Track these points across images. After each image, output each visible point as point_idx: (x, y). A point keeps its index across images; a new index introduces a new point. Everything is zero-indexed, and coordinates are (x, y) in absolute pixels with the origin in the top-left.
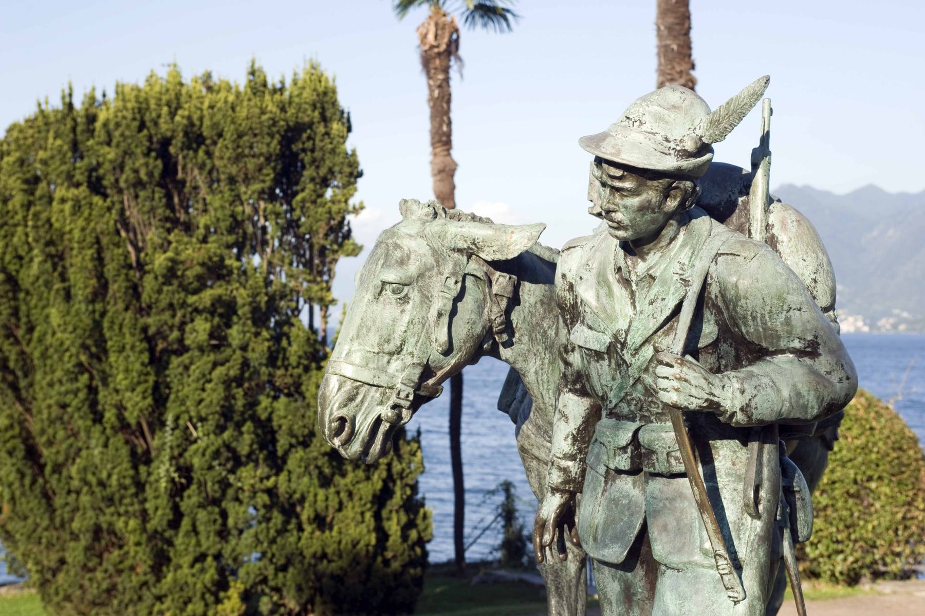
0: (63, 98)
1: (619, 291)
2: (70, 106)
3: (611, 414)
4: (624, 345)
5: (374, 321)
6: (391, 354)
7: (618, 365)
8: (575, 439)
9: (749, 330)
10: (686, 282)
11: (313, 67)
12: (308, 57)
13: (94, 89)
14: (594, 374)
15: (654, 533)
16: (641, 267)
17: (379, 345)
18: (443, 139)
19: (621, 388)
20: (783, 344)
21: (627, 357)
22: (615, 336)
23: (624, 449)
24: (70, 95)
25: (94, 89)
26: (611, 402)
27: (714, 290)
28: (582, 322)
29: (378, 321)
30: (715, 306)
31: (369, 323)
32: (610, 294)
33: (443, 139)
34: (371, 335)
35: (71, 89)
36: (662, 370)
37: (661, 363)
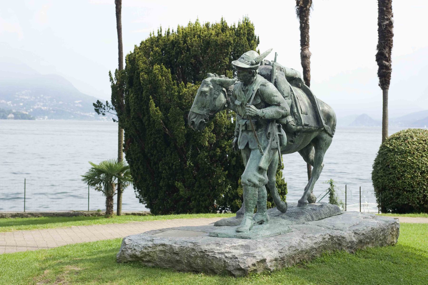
0: (158, 32)
1: (243, 93)
2: (160, 35)
6: (204, 107)
9: (266, 100)
10: (254, 91)
11: (246, 20)
12: (244, 16)
13: (169, 29)
18: (304, 42)
20: (273, 103)
22: (242, 102)
23: (244, 125)
24: (161, 31)
25: (169, 29)
27: (259, 92)
30: (260, 96)
32: (241, 93)
33: (304, 42)
35: (161, 29)
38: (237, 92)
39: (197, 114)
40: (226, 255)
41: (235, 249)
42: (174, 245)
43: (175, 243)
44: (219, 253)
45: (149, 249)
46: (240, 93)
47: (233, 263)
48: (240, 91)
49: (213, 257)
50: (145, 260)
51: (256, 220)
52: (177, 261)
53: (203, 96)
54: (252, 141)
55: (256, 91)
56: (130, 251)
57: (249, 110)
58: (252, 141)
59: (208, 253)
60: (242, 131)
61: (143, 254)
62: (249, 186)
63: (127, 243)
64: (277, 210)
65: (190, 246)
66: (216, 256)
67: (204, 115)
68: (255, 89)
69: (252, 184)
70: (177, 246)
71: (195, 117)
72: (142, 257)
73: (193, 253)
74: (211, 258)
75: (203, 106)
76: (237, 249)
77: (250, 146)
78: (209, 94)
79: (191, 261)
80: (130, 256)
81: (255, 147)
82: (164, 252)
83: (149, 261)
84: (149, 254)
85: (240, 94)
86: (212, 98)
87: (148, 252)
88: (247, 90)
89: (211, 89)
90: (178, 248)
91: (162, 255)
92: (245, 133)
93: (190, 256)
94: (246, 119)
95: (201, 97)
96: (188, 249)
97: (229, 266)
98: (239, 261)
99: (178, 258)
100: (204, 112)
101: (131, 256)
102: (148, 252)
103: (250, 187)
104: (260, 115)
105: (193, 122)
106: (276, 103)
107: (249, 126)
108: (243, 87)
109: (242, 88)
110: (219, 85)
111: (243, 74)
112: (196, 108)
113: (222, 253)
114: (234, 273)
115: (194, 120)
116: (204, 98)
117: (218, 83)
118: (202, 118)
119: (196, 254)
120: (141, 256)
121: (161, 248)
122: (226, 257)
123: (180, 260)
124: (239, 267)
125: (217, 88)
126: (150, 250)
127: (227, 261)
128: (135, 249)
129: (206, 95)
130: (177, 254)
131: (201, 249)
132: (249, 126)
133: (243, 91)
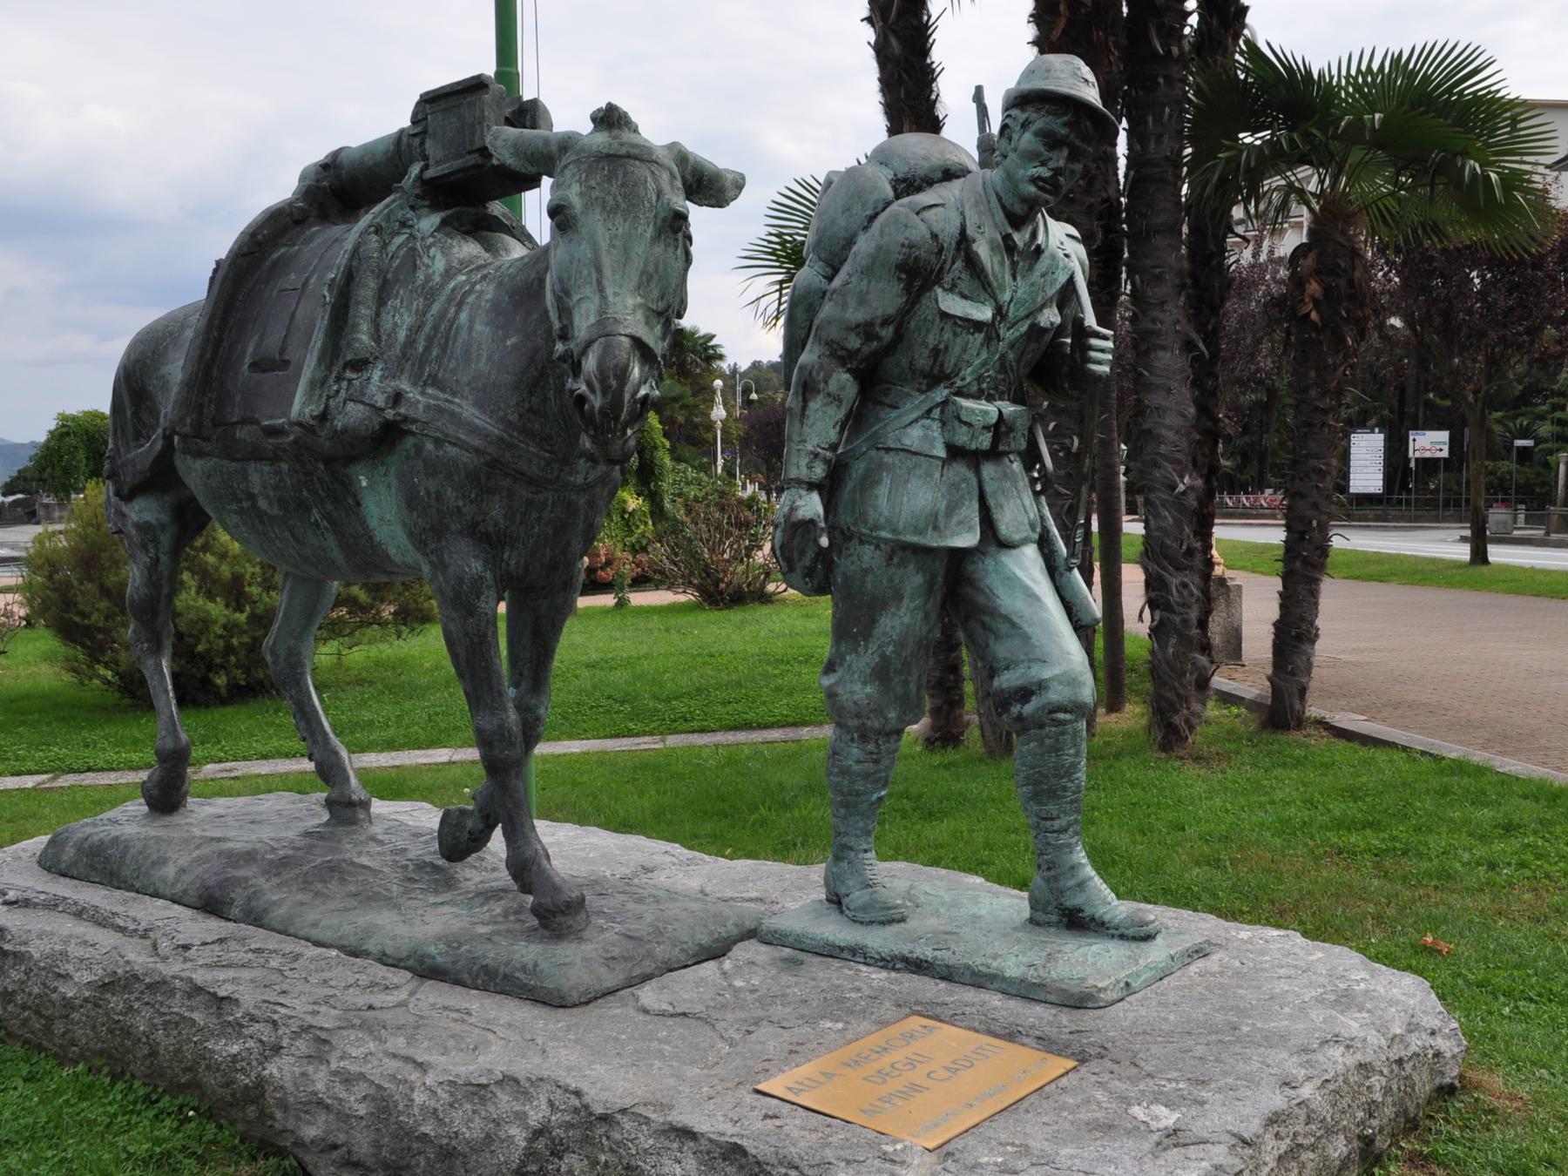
19: (983, 364)
21: (1001, 332)
26: (963, 379)
29: (661, 268)
31: (651, 269)
34: (653, 285)
95: (659, 249)
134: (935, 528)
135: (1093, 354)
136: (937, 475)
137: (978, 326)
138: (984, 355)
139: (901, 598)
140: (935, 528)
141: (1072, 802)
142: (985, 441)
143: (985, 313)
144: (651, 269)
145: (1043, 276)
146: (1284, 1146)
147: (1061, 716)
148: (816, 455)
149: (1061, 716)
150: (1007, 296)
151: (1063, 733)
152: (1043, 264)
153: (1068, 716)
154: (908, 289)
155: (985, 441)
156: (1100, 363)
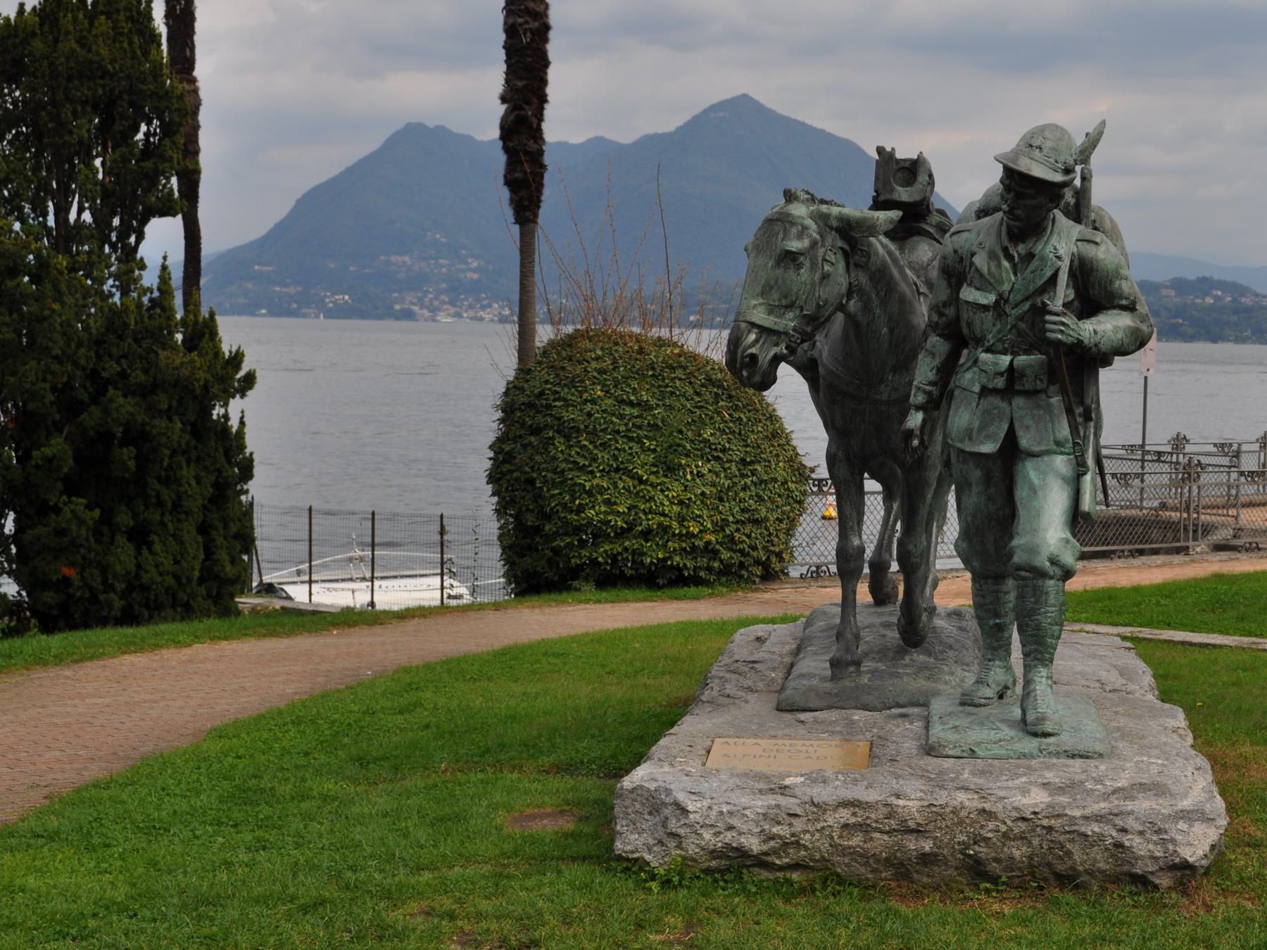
1: (1006, 264)
3: (988, 351)
4: (1007, 301)
5: (776, 282)
7: (999, 316)
8: (938, 370)
10: (1059, 258)
14: (978, 322)
15: (1020, 432)
16: (1022, 248)
17: (779, 300)
19: (1000, 331)
20: (1116, 302)
22: (1000, 296)
23: (1001, 374)
28: (970, 285)
31: (772, 283)
32: (999, 265)
36: (1048, 317)
37: (1051, 313)
38: (980, 261)
39: (763, 330)
40: (1119, 822)
41: (1125, 798)
42: (901, 802)
43: (898, 796)
44: (1085, 818)
45: (795, 821)
46: (993, 264)
47: (1151, 847)
48: (992, 256)
49: (1069, 832)
50: (778, 862)
51: (993, 686)
52: (926, 859)
53: (786, 268)
54: (1028, 428)
55: (1067, 262)
56: (707, 835)
57: (1063, 324)
58: (1028, 428)
59: (1045, 822)
60: (985, 391)
61: (772, 843)
62: (1052, 578)
63: (690, 808)
64: (897, 636)
65: (967, 803)
66: (1083, 829)
67: (786, 334)
68: (1061, 252)
69: (1058, 572)
70: (910, 803)
71: (756, 341)
72: (766, 854)
73: (991, 825)
74: (1062, 838)
75: (784, 302)
76: (1133, 798)
77: (1024, 442)
78: (807, 264)
79: (982, 850)
80: (713, 851)
81: (1044, 448)
82: (864, 828)
83: (795, 866)
84: (797, 843)
85: (993, 269)
86: (817, 277)
87: (793, 835)
88: (1030, 256)
89: (814, 244)
90: (918, 811)
91: (856, 841)
92: (995, 400)
93: (978, 839)
94: (1005, 353)
95: (779, 272)
96: (963, 814)
97: (1137, 858)
98: (1173, 841)
99: (927, 846)
100: (789, 322)
101: (714, 854)
102: (793, 835)
103: (1052, 582)
104: (1086, 342)
105: (754, 357)
106: (1124, 302)
107: (1023, 375)
108: (1006, 243)
109: (1005, 250)
110: (837, 230)
111: (1034, 202)
112: (761, 309)
113: (1099, 818)
114: (1158, 882)
115: (753, 350)
116: (791, 273)
117: (835, 224)
118: (777, 345)
119: (1003, 828)
120: (765, 848)
121: (845, 815)
122: (1124, 830)
123: (936, 855)
124: (1177, 860)
125: (829, 241)
126: (799, 825)
127: (1127, 844)
128: (731, 828)
129: (799, 266)
130: (917, 832)
131: (1016, 809)
132: (1023, 375)
133: (1009, 257)
134: (970, 439)
135: (1048, 326)
136: (974, 404)
137: (985, 308)
138: (999, 326)
139: (970, 485)
140: (970, 439)
141: (1032, 636)
142: (1000, 383)
143: (988, 299)
144: (772, 283)
145: (1032, 272)
146: (853, 820)
147: (1023, 573)
148: (919, 388)
149: (1023, 573)
150: (1006, 287)
151: (1026, 586)
152: (1035, 263)
153: (1028, 574)
154: (949, 285)
155: (1000, 383)
156: (1053, 331)
